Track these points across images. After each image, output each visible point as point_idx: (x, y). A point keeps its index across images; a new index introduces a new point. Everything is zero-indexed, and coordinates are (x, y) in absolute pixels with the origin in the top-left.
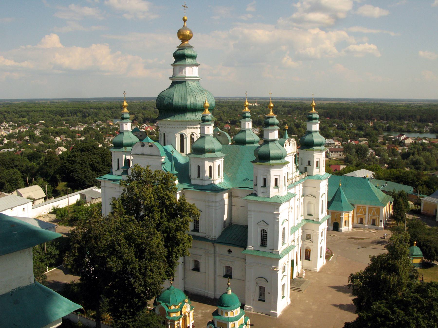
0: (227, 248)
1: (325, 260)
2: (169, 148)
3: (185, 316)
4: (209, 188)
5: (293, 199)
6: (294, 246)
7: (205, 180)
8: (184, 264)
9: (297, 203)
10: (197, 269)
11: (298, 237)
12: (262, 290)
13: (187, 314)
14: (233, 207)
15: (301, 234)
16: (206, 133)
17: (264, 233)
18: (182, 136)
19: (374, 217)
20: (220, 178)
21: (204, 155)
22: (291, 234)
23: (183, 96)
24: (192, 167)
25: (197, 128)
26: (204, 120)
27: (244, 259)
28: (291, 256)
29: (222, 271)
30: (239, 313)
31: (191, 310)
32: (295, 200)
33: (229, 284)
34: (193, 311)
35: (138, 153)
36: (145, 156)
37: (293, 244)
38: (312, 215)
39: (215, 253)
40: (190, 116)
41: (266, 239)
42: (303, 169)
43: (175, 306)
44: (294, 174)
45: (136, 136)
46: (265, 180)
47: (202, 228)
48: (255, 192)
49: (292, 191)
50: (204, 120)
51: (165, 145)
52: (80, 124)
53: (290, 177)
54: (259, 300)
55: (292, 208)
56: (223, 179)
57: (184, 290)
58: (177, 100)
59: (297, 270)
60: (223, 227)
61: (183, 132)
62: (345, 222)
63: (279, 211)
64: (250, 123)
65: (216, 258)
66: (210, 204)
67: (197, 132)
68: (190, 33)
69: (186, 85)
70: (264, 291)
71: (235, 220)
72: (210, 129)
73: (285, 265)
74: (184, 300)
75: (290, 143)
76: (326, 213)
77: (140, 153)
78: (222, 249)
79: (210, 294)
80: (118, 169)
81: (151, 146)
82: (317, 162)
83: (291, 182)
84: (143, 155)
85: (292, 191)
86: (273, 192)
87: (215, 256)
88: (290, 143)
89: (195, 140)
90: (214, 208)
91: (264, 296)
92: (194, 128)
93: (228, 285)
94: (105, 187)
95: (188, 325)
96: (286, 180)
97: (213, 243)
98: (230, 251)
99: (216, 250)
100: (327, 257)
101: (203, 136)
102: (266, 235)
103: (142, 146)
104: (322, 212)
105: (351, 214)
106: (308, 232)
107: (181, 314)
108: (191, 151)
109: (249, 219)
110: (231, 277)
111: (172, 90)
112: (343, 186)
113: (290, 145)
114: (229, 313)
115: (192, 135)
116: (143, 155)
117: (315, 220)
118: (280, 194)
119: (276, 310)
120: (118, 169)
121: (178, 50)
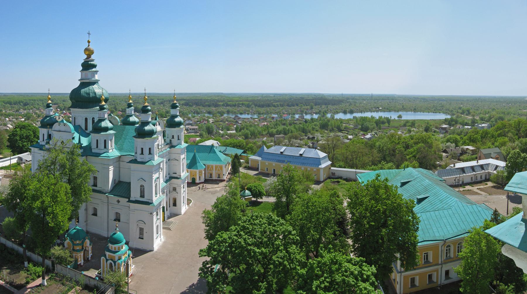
0: (117, 198)
8: (87, 210)
10: (95, 214)
13: (87, 249)
14: (121, 169)
18: (86, 119)
27: (128, 207)
29: (113, 216)
31: (90, 245)
38: (176, 174)
39: (108, 203)
41: (144, 191)
46: (142, 149)
48: (136, 158)
62: (200, 177)
65: (109, 206)
71: (124, 179)
87: (108, 205)
89: (95, 122)
93: (117, 226)
98: (119, 201)
99: (109, 200)
106: (175, 186)
110: (119, 220)
115: (93, 118)
117: (178, 177)
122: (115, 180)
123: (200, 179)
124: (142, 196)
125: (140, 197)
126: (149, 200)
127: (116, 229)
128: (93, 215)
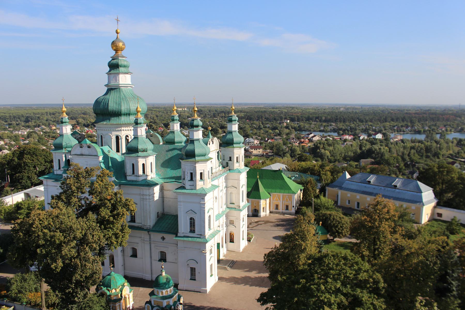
0: (161, 235)
1: (247, 242)
2: (106, 148)
3: (125, 298)
4: (143, 183)
5: (217, 189)
6: (220, 231)
7: (139, 176)
9: (221, 194)
10: (134, 255)
11: (223, 223)
12: (193, 270)
13: (127, 296)
14: (165, 199)
15: (225, 221)
16: (139, 134)
17: (193, 221)
18: (117, 138)
19: (287, 204)
20: (153, 173)
21: (137, 154)
22: (216, 221)
23: (117, 102)
24: (127, 165)
25: (131, 130)
26: (136, 123)
28: (218, 239)
29: (157, 256)
31: (130, 292)
32: (218, 191)
33: (163, 267)
34: (132, 293)
35: (78, 154)
36: (84, 156)
37: (218, 229)
38: (234, 204)
39: (150, 241)
40: (123, 119)
42: (225, 164)
44: (218, 169)
45: (75, 138)
46: (191, 174)
47: (137, 220)
48: (184, 185)
49: (215, 182)
50: (136, 123)
51: (102, 146)
52: (23, 129)
53: (214, 171)
54: (191, 279)
55: (216, 198)
56: (155, 175)
57: (123, 275)
58: (112, 106)
59: (223, 251)
60: (157, 216)
61: (118, 133)
62: (263, 208)
63: (205, 202)
64: (178, 125)
66: (145, 197)
67: (131, 134)
68: (123, 45)
69: (120, 91)
70: (195, 272)
72: (142, 131)
74: (124, 284)
75: (213, 142)
76: (246, 201)
77: (79, 153)
78: (157, 237)
79: (148, 277)
80: (60, 168)
82: (237, 157)
83: (214, 175)
84: (82, 155)
85: (215, 182)
86: (199, 184)
88: (213, 142)
89: (129, 141)
90: (148, 200)
91: (195, 275)
93: (162, 268)
94: (47, 185)
95: (128, 306)
96: (210, 174)
97: (148, 232)
98: (163, 238)
100: (249, 240)
101: (136, 138)
102: (194, 222)
103: (81, 147)
104: (243, 201)
105: (268, 200)
106: (231, 218)
108: (126, 151)
109: (179, 209)
111: (107, 96)
112: (260, 178)
113: (213, 144)
116: (82, 155)
117: (237, 207)
118: (204, 187)
119: (206, 287)
120: (60, 168)
121: (112, 60)
122: (158, 213)
125: (190, 232)
126: (201, 235)
127: (162, 271)
128: (131, 256)
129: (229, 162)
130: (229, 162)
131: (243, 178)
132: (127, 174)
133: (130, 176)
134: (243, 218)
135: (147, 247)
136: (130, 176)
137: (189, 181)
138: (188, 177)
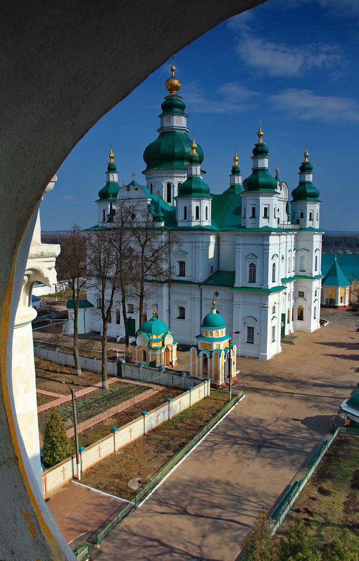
3: (167, 349)
10: (182, 317)
12: (251, 330)
13: (169, 347)
15: (293, 291)
18: (169, 185)
20: (208, 220)
30: (224, 335)
38: (305, 271)
40: (176, 164)
41: (255, 274)
43: (157, 335)
46: (254, 209)
54: (247, 342)
55: (283, 258)
56: (210, 223)
58: (164, 147)
61: (169, 180)
62: (341, 298)
66: (197, 244)
70: (253, 333)
71: (223, 267)
73: (275, 305)
76: (320, 272)
81: (136, 189)
82: (310, 214)
86: (263, 223)
90: (200, 248)
91: (253, 338)
92: (181, 177)
107: (163, 345)
113: (281, 190)
114: (214, 332)
115: (179, 184)
117: (308, 275)
118: (269, 225)
119: (266, 352)
122: (212, 267)
123: (341, 302)
124: (252, 279)
129: (301, 219)
130: (301, 219)
131: (317, 240)
132: (178, 220)
133: (181, 221)
134: (316, 291)
135: (198, 304)
136: (181, 221)
137: (251, 217)
138: (249, 213)
